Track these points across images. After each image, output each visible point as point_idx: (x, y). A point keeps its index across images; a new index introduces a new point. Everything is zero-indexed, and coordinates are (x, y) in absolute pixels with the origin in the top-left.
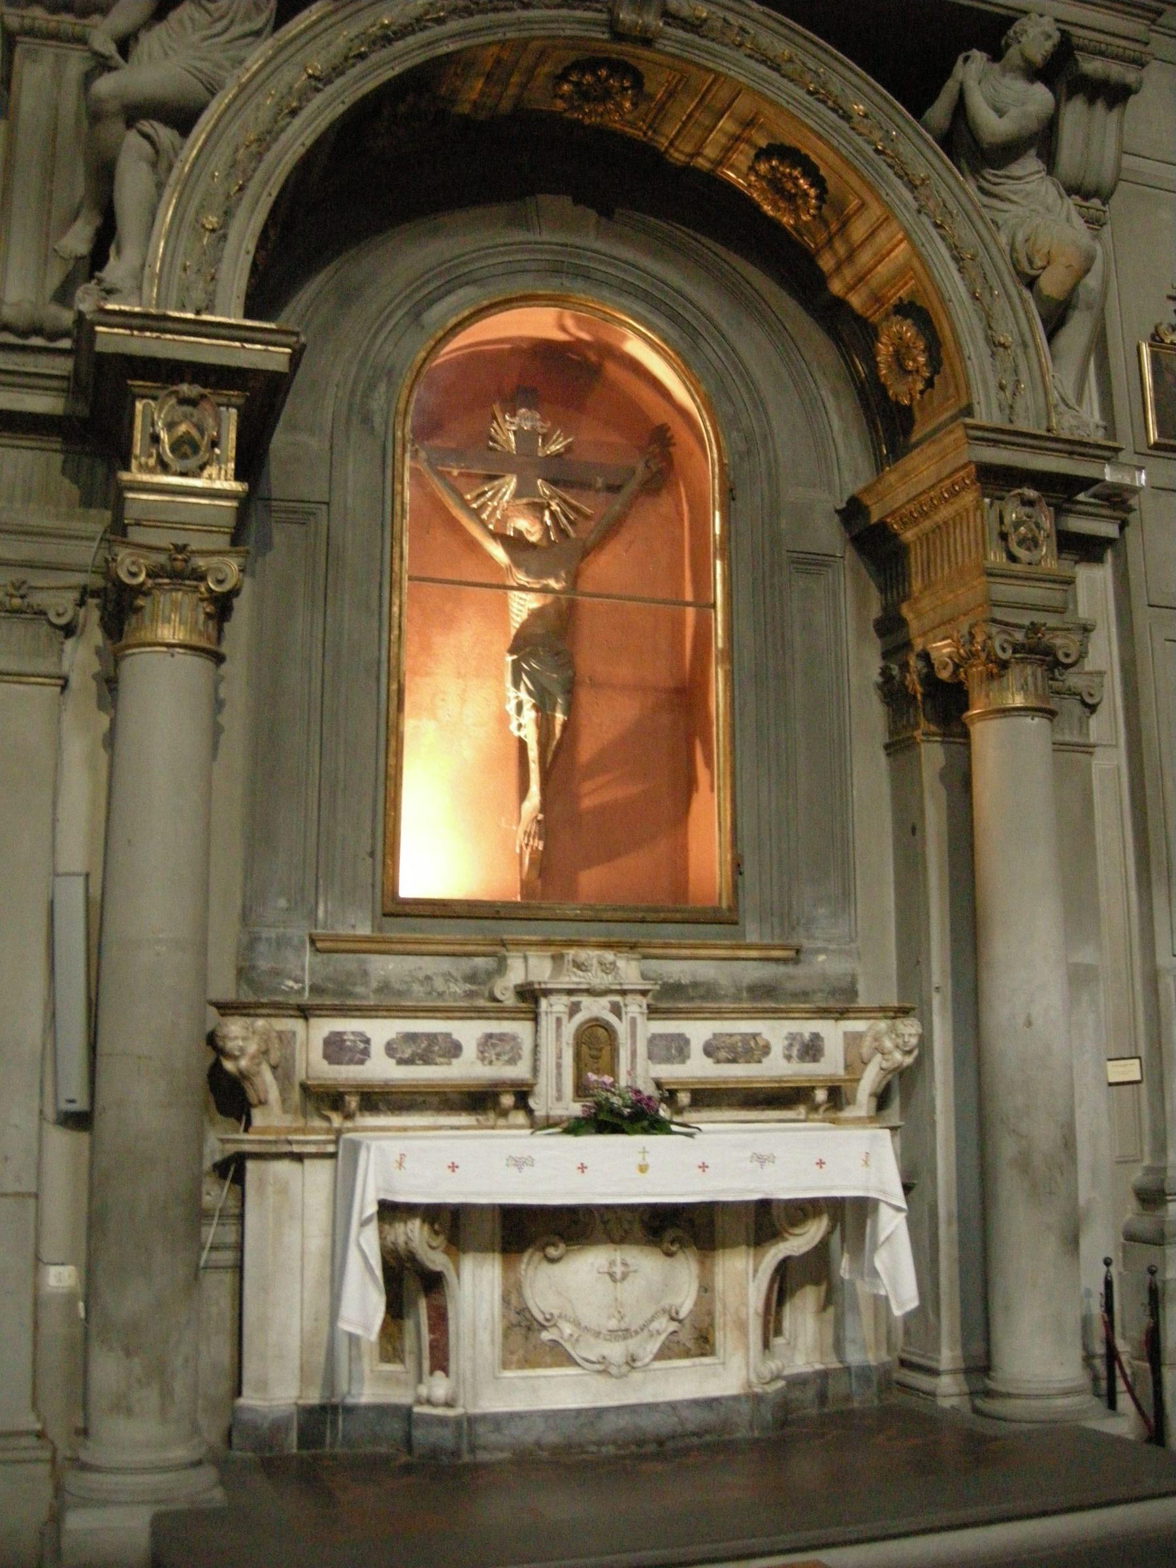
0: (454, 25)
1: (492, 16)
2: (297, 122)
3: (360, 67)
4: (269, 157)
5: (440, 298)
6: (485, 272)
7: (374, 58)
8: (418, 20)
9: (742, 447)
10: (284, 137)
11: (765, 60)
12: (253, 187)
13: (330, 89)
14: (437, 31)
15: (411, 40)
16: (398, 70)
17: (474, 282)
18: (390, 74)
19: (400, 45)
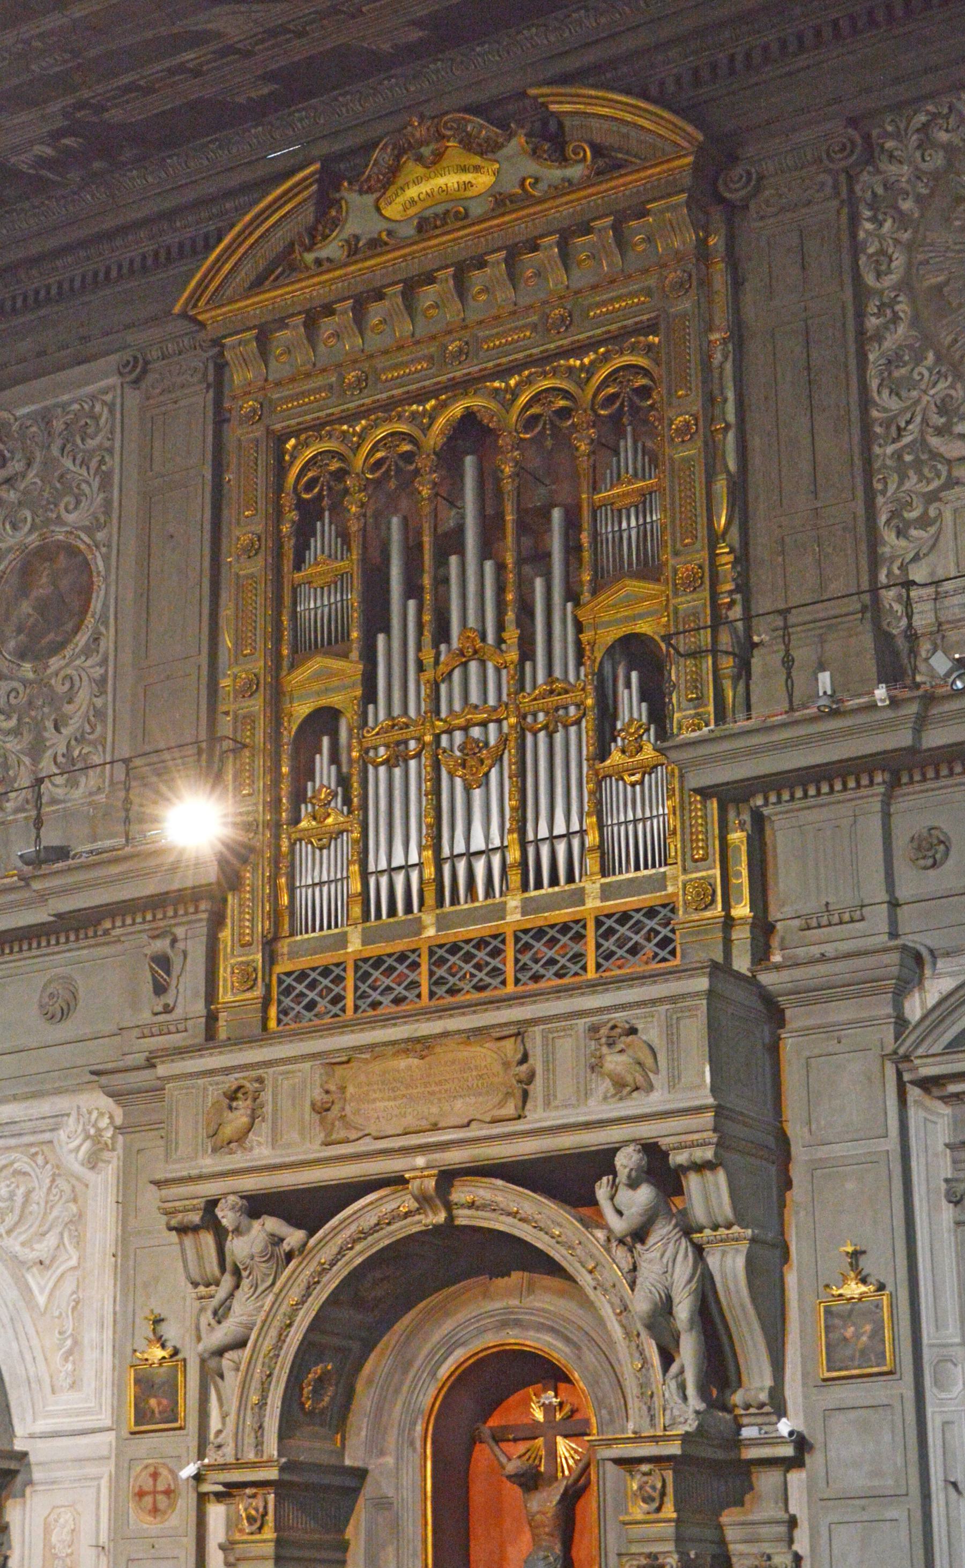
0: (358, 1247)
1: (376, 1235)
2: (293, 1329)
3: (319, 1287)
4: (282, 1353)
5: (446, 1358)
6: (467, 1336)
7: (324, 1280)
8: (339, 1253)
9: (607, 1417)
10: (288, 1340)
11: (509, 1214)
12: (276, 1372)
13: (306, 1305)
14: (351, 1254)
15: (340, 1263)
16: (337, 1282)
17: (463, 1344)
18: (334, 1285)
19: (335, 1268)
